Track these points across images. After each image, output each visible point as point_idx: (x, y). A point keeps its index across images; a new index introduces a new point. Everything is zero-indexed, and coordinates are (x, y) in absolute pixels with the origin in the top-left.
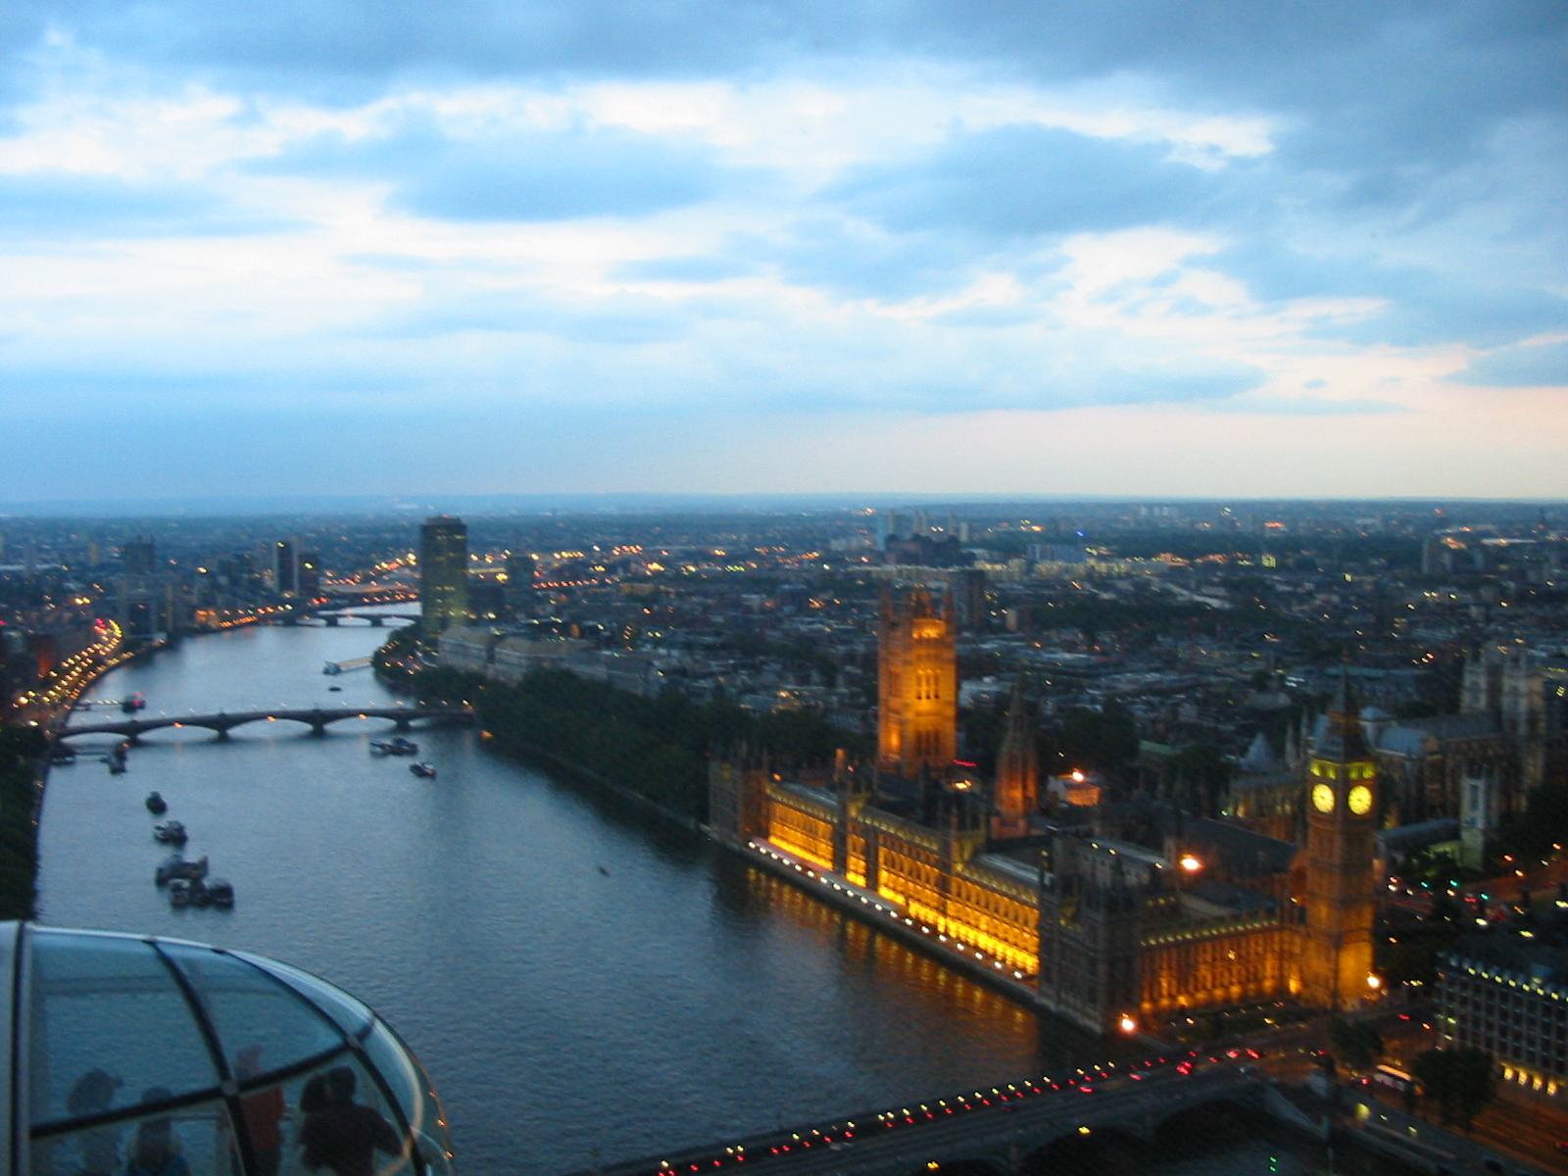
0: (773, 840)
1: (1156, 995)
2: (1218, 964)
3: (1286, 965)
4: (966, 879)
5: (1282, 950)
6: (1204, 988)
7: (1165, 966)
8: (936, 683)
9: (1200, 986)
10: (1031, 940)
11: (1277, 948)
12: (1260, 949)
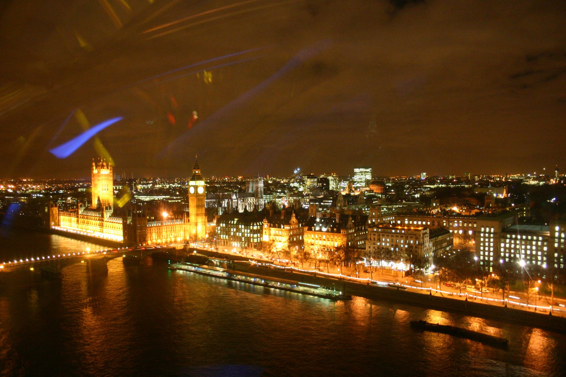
1: (152, 239)
2: (168, 232)
3: (186, 233)
4: (108, 222)
5: (184, 230)
6: (165, 238)
7: (154, 232)
8: (108, 186)
10: (121, 232)
11: (183, 229)
12: (179, 229)
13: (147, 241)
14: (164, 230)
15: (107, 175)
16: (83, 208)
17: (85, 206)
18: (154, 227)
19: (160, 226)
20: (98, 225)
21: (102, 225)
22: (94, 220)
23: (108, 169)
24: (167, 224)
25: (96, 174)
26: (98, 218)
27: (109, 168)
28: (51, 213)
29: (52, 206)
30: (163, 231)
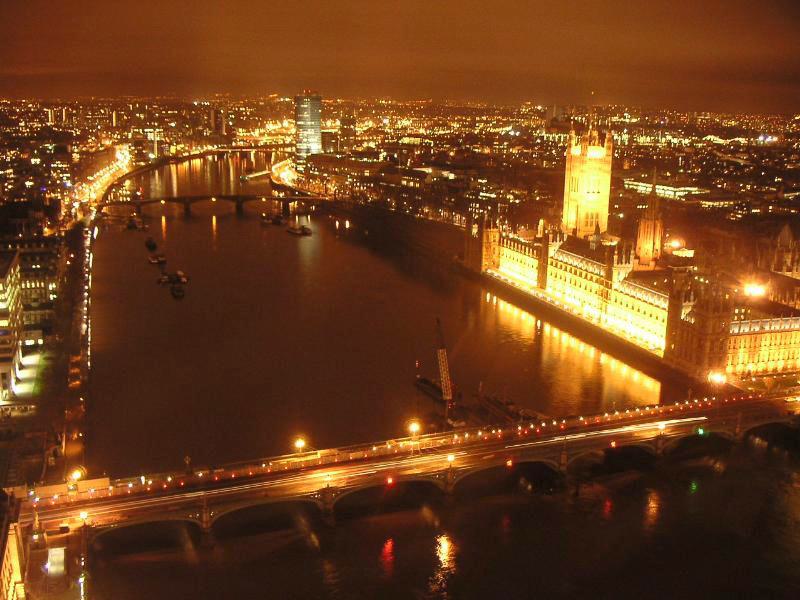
0: (501, 269)
9: (761, 360)
13: (725, 368)
14: (766, 340)
15: (601, 160)
16: (558, 244)
17: (562, 238)
18: (744, 334)
19: (758, 333)
20: (594, 291)
21: (605, 296)
22: (586, 277)
23: (603, 146)
24: (773, 328)
25: (576, 158)
26: (595, 277)
27: (606, 144)
28: (485, 240)
29: (489, 226)
30: (763, 345)
